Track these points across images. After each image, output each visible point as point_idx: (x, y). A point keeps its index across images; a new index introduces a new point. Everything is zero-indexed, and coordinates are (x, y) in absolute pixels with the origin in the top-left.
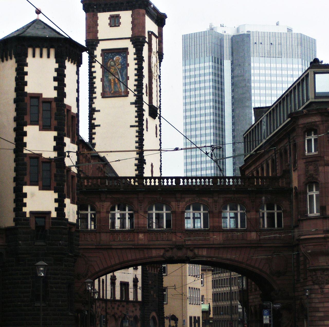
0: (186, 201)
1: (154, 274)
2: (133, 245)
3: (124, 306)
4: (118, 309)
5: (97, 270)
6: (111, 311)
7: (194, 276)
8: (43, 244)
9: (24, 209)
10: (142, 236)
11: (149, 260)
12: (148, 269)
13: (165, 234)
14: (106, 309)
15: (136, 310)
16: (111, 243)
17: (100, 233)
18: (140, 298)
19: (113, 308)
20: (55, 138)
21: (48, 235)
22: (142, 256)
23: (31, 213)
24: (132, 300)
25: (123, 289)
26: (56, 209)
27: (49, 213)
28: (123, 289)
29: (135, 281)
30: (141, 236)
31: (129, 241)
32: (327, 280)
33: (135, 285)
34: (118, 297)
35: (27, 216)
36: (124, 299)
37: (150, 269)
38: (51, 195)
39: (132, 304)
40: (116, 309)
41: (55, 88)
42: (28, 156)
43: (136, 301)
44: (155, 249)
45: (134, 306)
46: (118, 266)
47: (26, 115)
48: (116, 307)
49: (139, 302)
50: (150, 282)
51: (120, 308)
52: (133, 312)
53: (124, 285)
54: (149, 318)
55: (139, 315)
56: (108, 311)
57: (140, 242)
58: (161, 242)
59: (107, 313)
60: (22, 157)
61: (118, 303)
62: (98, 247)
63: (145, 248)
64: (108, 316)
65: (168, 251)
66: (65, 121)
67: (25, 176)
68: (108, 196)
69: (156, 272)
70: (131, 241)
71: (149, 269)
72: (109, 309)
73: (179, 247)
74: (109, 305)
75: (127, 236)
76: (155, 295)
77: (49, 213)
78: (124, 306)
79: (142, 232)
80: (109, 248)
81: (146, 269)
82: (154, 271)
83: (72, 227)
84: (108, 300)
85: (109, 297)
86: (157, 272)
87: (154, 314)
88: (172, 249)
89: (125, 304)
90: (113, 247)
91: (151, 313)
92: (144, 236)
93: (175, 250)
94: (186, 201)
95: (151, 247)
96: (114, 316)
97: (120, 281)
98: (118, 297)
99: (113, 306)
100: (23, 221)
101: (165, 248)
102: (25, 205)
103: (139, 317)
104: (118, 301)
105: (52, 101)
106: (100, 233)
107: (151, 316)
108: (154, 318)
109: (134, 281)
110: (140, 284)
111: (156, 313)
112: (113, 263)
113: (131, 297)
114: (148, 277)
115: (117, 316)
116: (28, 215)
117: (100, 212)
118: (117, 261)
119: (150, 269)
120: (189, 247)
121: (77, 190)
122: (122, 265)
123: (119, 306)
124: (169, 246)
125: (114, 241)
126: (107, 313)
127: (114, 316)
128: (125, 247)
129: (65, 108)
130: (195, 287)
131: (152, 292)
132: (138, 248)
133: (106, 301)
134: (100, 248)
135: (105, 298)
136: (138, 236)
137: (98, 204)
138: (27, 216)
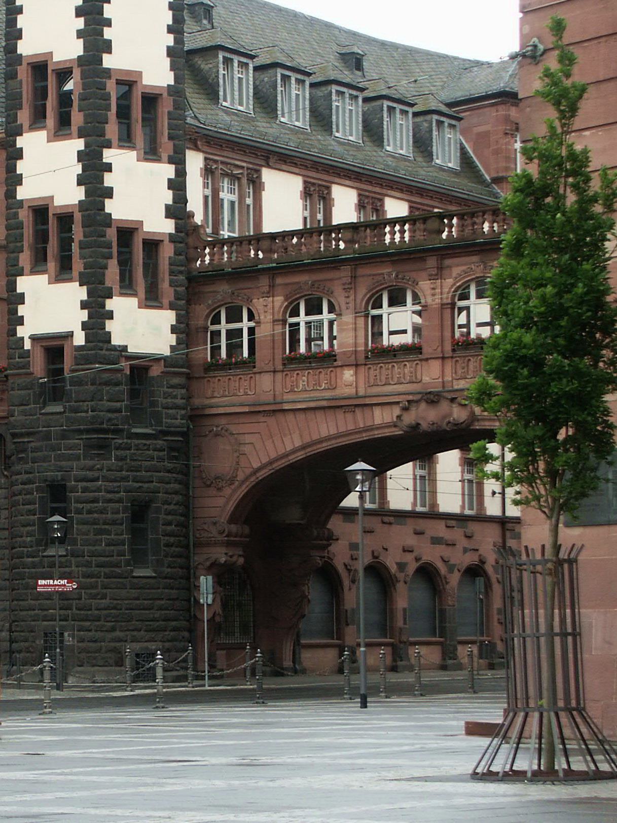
0: (454, 275)
5: (256, 465)
8: (59, 409)
9: (21, 331)
10: (352, 376)
11: (365, 436)
13: (405, 365)
20: (81, 156)
21: (69, 387)
22: (351, 427)
23: (34, 339)
26: (85, 326)
27: (70, 335)
35: (26, 348)
38: (76, 292)
41: (80, 34)
42: (26, 206)
47: (21, 109)
58: (395, 387)
60: (14, 210)
62: (253, 409)
65: (405, 409)
66: (108, 108)
67: (21, 254)
68: (279, 281)
73: (432, 398)
77: (70, 335)
80: (276, 411)
88: (417, 402)
90: (286, 407)
92: (356, 373)
93: (423, 405)
94: (454, 275)
95: (368, 401)
100: (19, 358)
101: (398, 403)
102: (21, 321)
105: (72, 67)
112: (289, 447)
116: (27, 345)
117: (258, 323)
118: (298, 443)
121: (172, 273)
124: (411, 398)
125: (292, 391)
128: (312, 405)
129: (110, 78)
134: (259, 412)
137: (258, 304)
138: (26, 348)
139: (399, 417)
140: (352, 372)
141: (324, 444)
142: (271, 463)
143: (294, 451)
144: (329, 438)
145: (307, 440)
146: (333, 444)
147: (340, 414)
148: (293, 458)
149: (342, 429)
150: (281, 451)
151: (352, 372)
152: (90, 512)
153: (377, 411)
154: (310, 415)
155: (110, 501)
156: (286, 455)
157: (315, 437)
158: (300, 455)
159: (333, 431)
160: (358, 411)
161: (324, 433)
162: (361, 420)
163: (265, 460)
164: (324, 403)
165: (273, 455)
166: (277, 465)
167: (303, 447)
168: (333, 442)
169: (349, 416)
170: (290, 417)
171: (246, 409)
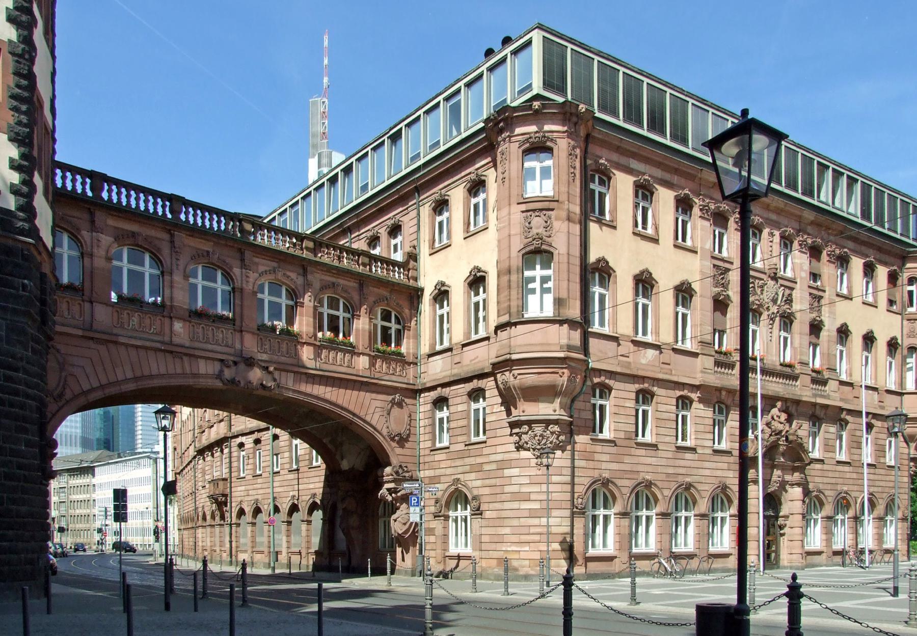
22: (179, 371)
32: (551, 443)
63: (186, 355)
65: (228, 367)
93: (242, 366)
112: (120, 377)
118: (129, 375)
122: (139, 383)
128: (148, 344)
132: (171, 352)
139: (221, 371)
143: (126, 380)
150: (112, 379)
152: (12, 405)
153: (202, 363)
154: (142, 353)
155: (28, 396)
156: (117, 383)
159: (163, 371)
160: (185, 359)
167: (136, 379)
169: (177, 361)
170: (122, 350)
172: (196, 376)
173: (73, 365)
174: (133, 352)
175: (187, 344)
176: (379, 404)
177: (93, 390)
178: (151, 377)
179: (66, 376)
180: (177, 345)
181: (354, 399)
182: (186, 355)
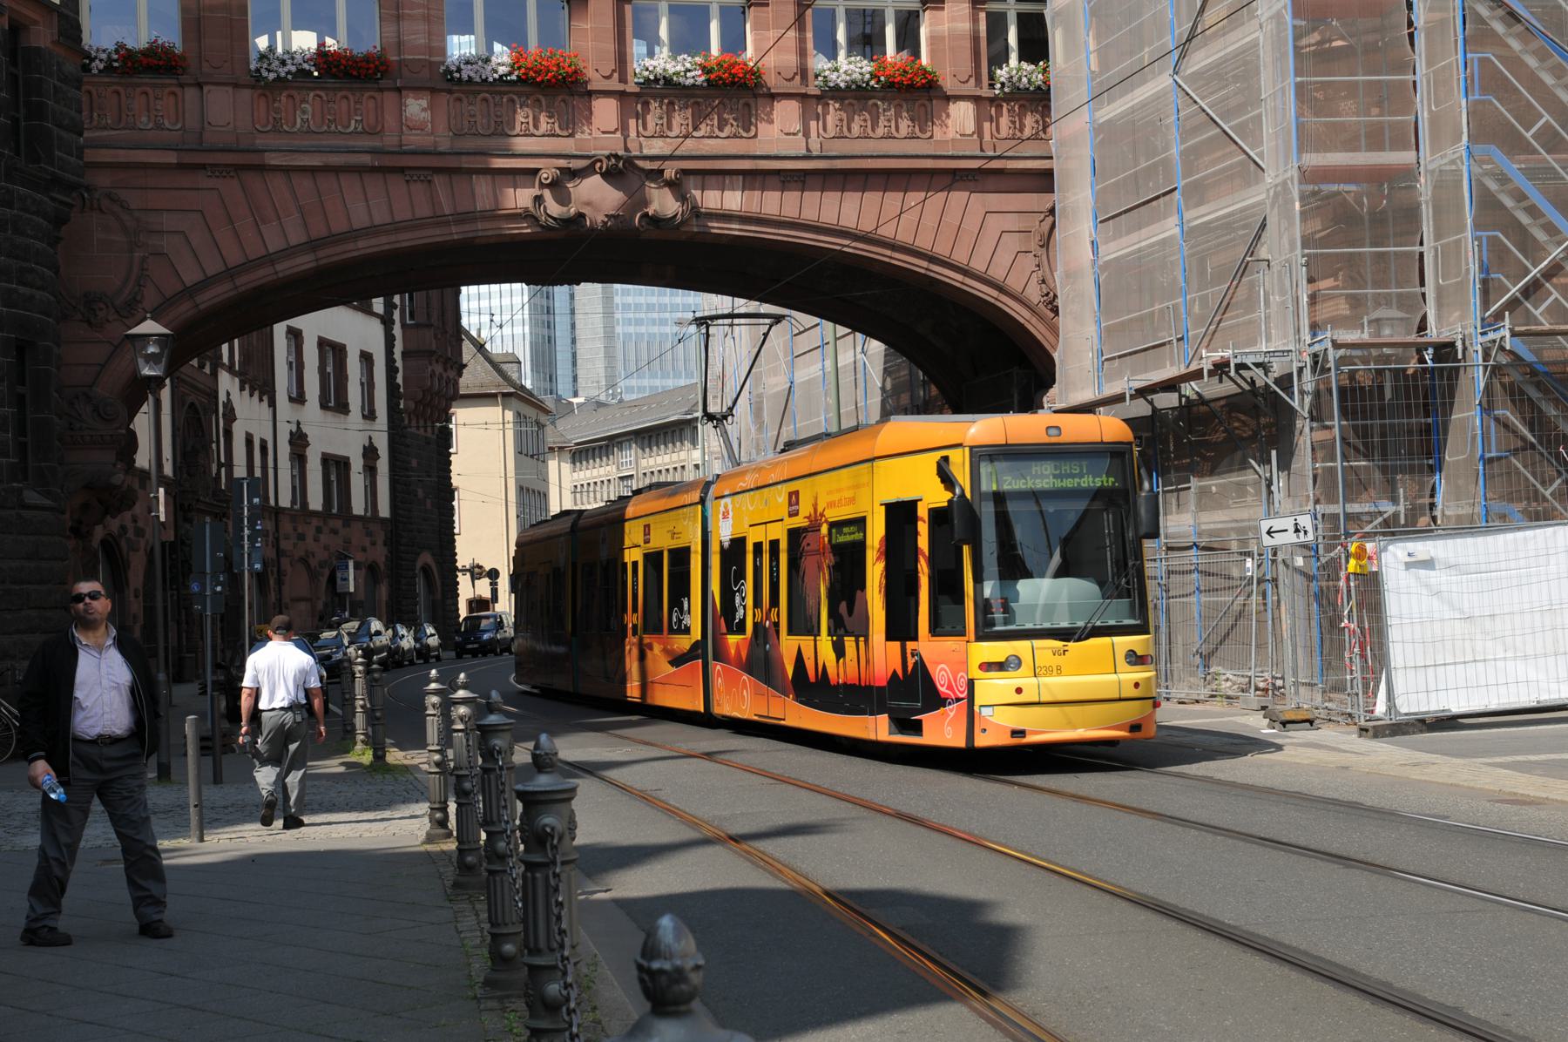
1: (426, 438)
2: (372, 151)
3: (335, 532)
4: (316, 540)
5: (190, 276)
6: (295, 545)
7: (532, 456)
10: (424, 110)
11: (456, 233)
12: (406, 422)
14: (277, 539)
15: (373, 544)
16: (260, 142)
17: (200, 86)
18: (384, 510)
19: (302, 537)
22: (424, 211)
24: (362, 513)
25: (333, 477)
28: (333, 477)
29: (370, 453)
30: (416, 107)
31: (355, 132)
33: (370, 470)
34: (316, 502)
36: (335, 511)
37: (414, 423)
39: (359, 525)
40: (309, 540)
43: (372, 517)
44: (489, 177)
45: (369, 534)
46: (299, 260)
48: (310, 533)
49: (384, 520)
50: (414, 463)
51: (323, 538)
52: (364, 550)
53: (336, 466)
54: (414, 570)
55: (383, 559)
56: (284, 545)
57: (414, 140)
59: (280, 553)
61: (315, 522)
62: (189, 159)
63: (438, 170)
64: (285, 562)
69: (429, 434)
70: (364, 132)
71: (410, 420)
72: (287, 539)
74: (287, 526)
75: (344, 103)
76: (429, 501)
78: (335, 532)
79: (417, 89)
81: (403, 421)
82: (426, 431)
83: (36, 23)
84: (285, 509)
85: (285, 501)
86: (433, 433)
87: (426, 558)
89: (338, 524)
90: (274, 160)
91: (418, 554)
92: (431, 107)
95: (466, 162)
96: (304, 561)
97: (323, 454)
98: (316, 502)
99: (300, 531)
103: (382, 567)
104: (315, 513)
106: (200, 86)
107: (419, 564)
108: (426, 570)
109: (364, 456)
110: (383, 465)
111: (433, 555)
112: (274, 244)
113: (358, 506)
114: (408, 446)
115: (313, 563)
118: (296, 237)
119: (414, 423)
120: (655, 165)
122: (321, 254)
123: (319, 530)
125: (277, 130)
126: (280, 553)
127: (304, 561)
130: (536, 489)
131: (420, 493)
132: (402, 170)
133: (278, 511)
134: (203, 167)
135: (272, 502)
136: (401, 107)
140: (424, 103)
141: (361, 244)
142: (230, 273)
143: (289, 252)
144: (372, 230)
145: (319, 230)
146: (383, 243)
147: (397, 185)
148: (285, 268)
149: (403, 214)
150: (254, 251)
151: (424, 103)
156: (269, 259)
157: (339, 226)
158: (304, 262)
159: (380, 217)
160: (438, 180)
161: (360, 219)
162: (445, 196)
163: (214, 267)
164: (366, 159)
165: (234, 257)
166: (246, 281)
167: (313, 245)
168: (383, 239)
169: (418, 189)
170: (277, 183)
171: (172, 158)
172: (493, 215)
173: (161, 232)
174: (304, 184)
175: (444, 146)
176: (1012, 222)
177: (206, 283)
178: (353, 235)
179: (144, 259)
180: (414, 153)
181: (930, 220)
182: (438, 170)
